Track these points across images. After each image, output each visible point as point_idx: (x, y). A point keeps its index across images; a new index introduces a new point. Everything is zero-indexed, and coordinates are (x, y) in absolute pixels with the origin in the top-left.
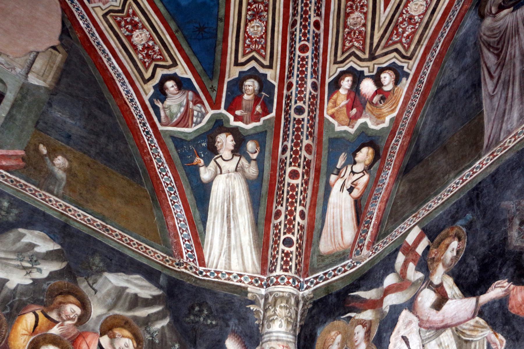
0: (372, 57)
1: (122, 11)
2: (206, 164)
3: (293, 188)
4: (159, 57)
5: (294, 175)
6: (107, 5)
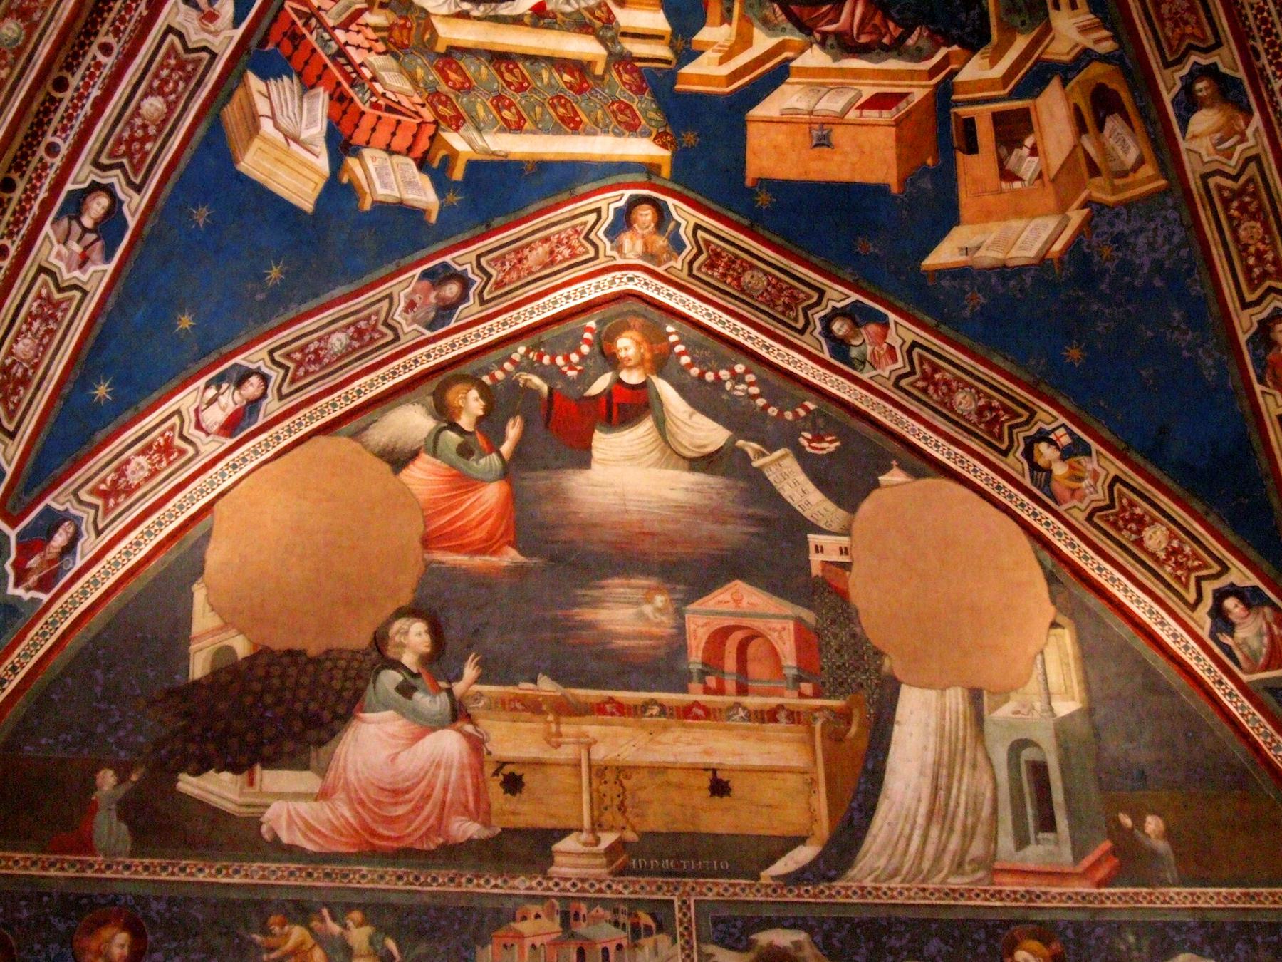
1: (1111, 506)
4: (1196, 563)
6: (1087, 501)
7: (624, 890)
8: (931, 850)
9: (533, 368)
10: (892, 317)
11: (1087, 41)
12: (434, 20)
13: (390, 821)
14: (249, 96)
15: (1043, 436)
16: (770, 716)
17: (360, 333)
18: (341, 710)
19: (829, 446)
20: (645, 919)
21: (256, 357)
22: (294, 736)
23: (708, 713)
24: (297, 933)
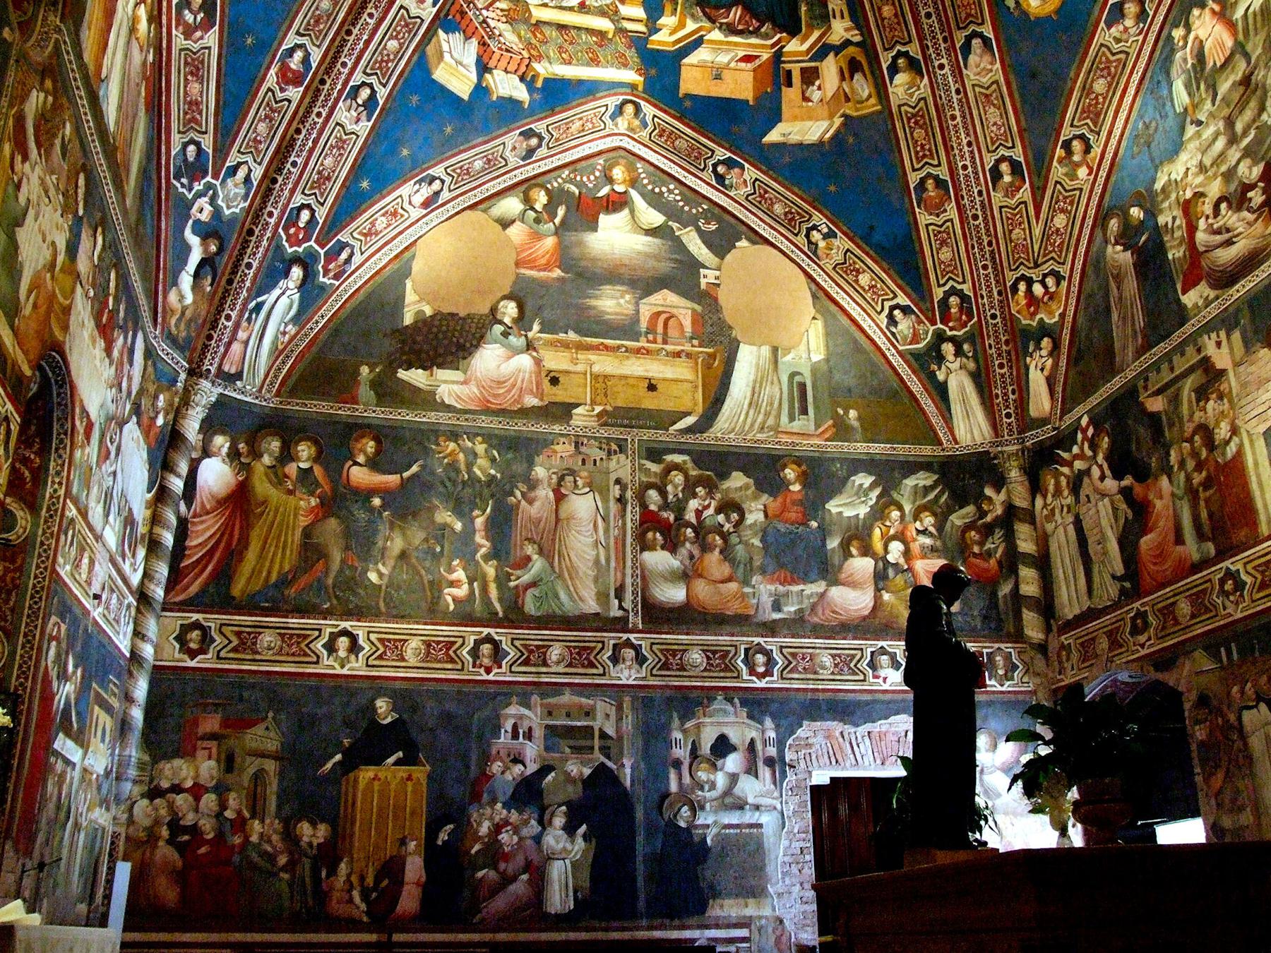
0: (1037, 265)
2: (940, 369)
3: (1003, 376)
5: (1001, 366)
7: (604, 433)
8: (749, 421)
9: (571, 182)
10: (747, 165)
11: (848, 36)
12: (531, 8)
13: (495, 396)
14: (439, 42)
15: (815, 227)
16: (678, 355)
17: (489, 161)
18: (475, 343)
19: (713, 227)
20: (614, 447)
21: (438, 171)
22: (452, 354)
23: (648, 352)
24: (452, 445)
